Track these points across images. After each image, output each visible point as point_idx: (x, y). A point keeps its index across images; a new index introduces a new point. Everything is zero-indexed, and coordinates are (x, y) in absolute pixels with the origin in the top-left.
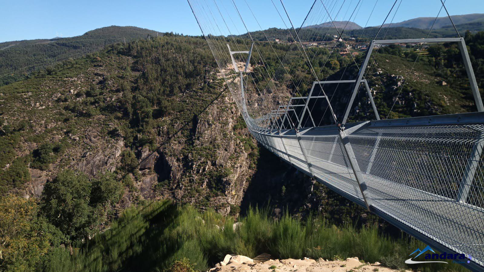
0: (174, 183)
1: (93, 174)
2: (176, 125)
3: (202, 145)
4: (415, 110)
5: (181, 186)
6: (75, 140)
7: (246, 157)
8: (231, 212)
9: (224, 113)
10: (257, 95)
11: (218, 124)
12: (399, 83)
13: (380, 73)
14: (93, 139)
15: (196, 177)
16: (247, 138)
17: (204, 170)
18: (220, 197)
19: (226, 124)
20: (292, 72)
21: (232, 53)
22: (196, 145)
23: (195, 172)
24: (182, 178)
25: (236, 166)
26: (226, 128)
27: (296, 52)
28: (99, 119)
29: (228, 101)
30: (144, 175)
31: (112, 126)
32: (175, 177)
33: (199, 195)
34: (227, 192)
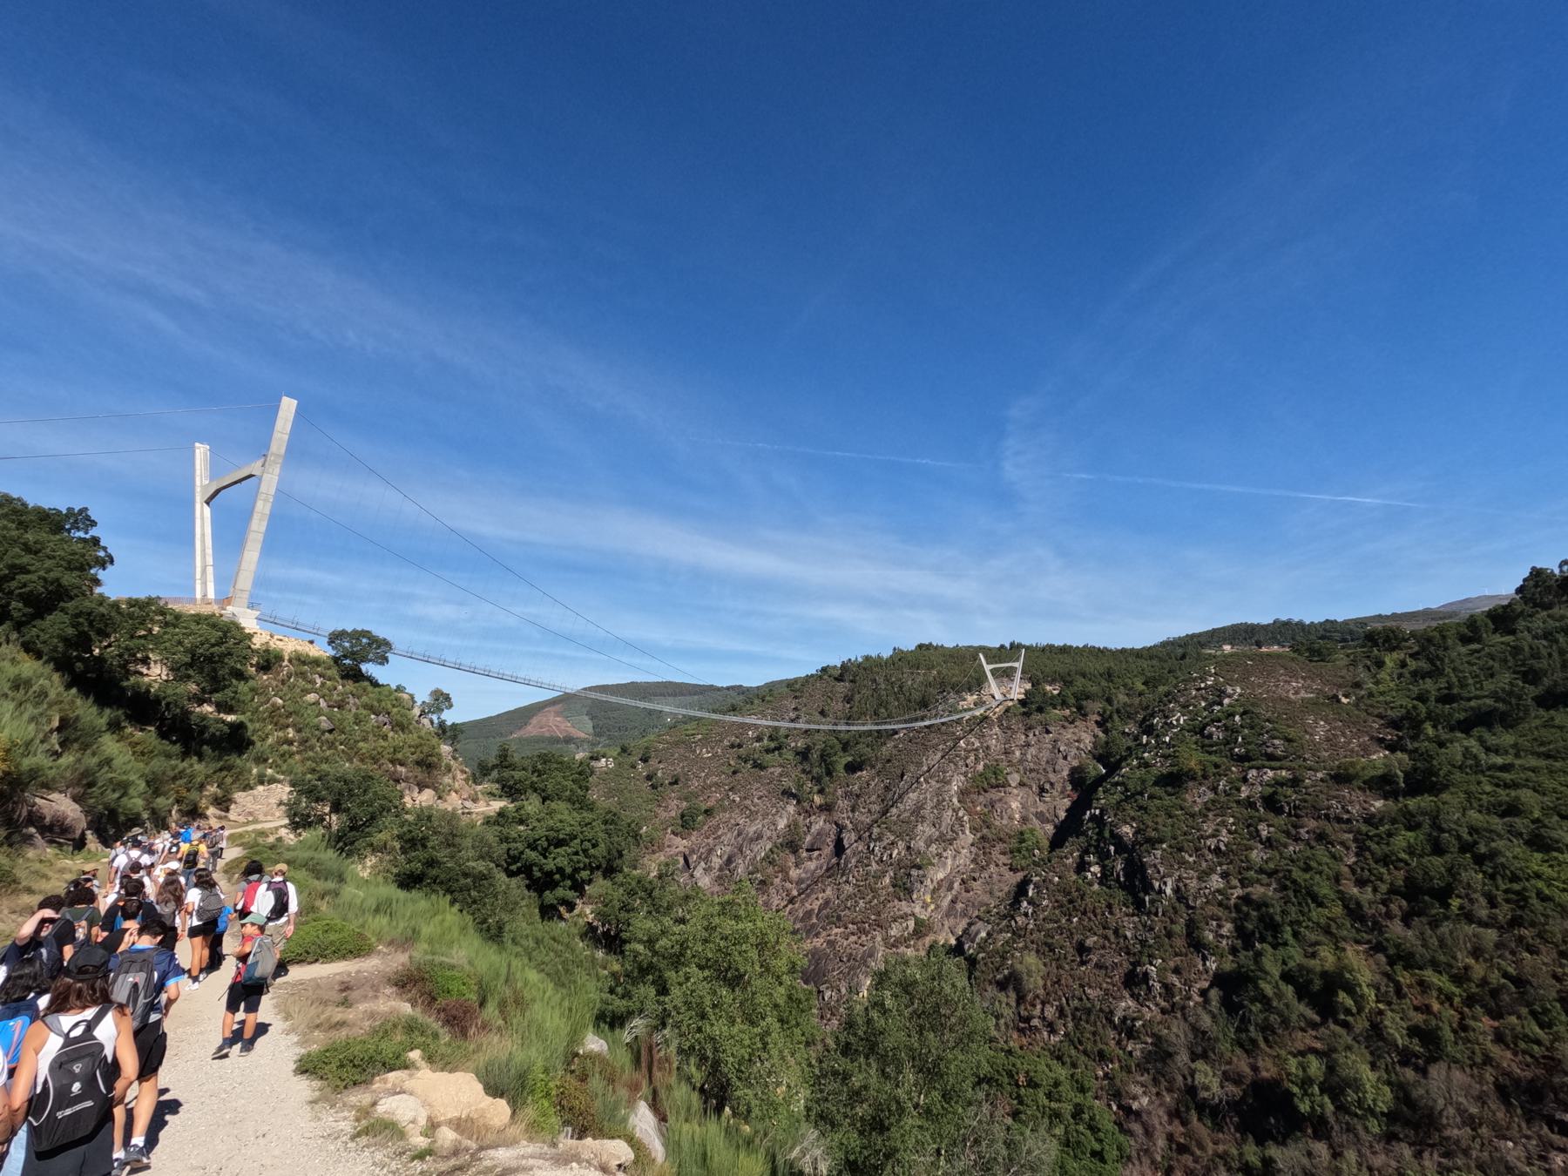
0: (842, 876)
1: (742, 852)
2: (873, 784)
3: (899, 815)
5: (851, 878)
6: (734, 801)
7: (970, 841)
8: (915, 930)
9: (951, 765)
10: (1023, 737)
11: (934, 783)
12: (1226, 701)
14: (756, 800)
15: (875, 866)
16: (986, 810)
17: (891, 855)
18: (904, 903)
19: (949, 783)
20: (1109, 701)
21: (988, 668)
23: (877, 859)
24: (856, 867)
25: (945, 854)
26: (946, 789)
28: (772, 773)
30: (810, 859)
31: (787, 783)
32: (846, 865)
33: (874, 897)
34: (915, 896)
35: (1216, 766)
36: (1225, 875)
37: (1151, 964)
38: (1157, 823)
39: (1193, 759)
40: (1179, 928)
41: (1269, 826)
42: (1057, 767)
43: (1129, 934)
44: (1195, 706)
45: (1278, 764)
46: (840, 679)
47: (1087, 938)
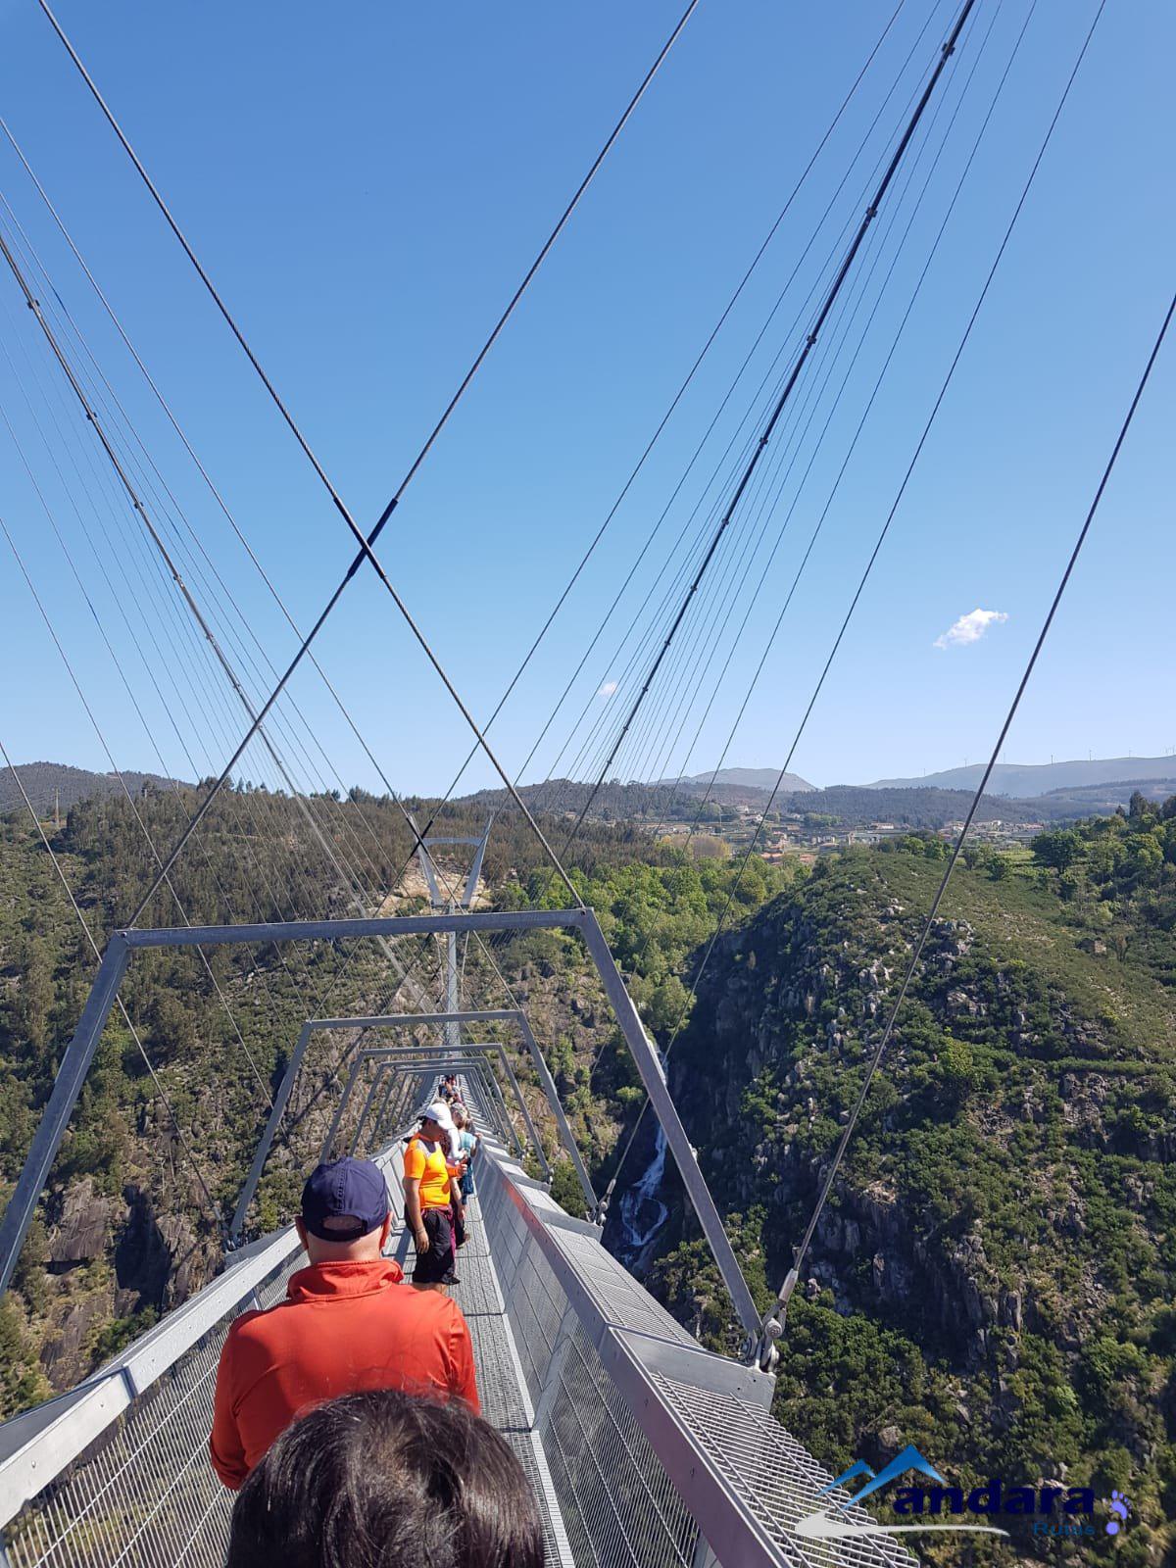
3: (298, 1166)
4: (1024, 1036)
12: (961, 945)
13: (896, 911)
20: (618, 910)
22: (276, 1167)
27: (628, 847)
29: (404, 1000)
30: (65, 1289)
35: (1001, 1065)
36: (1108, 1278)
37: (1048, 1476)
38: (944, 1180)
39: (960, 1055)
40: (1068, 1394)
41: (1143, 1179)
42: (578, 1040)
43: (964, 1411)
44: (898, 950)
45: (1110, 1065)
46: (60, 844)
47: (880, 1430)
